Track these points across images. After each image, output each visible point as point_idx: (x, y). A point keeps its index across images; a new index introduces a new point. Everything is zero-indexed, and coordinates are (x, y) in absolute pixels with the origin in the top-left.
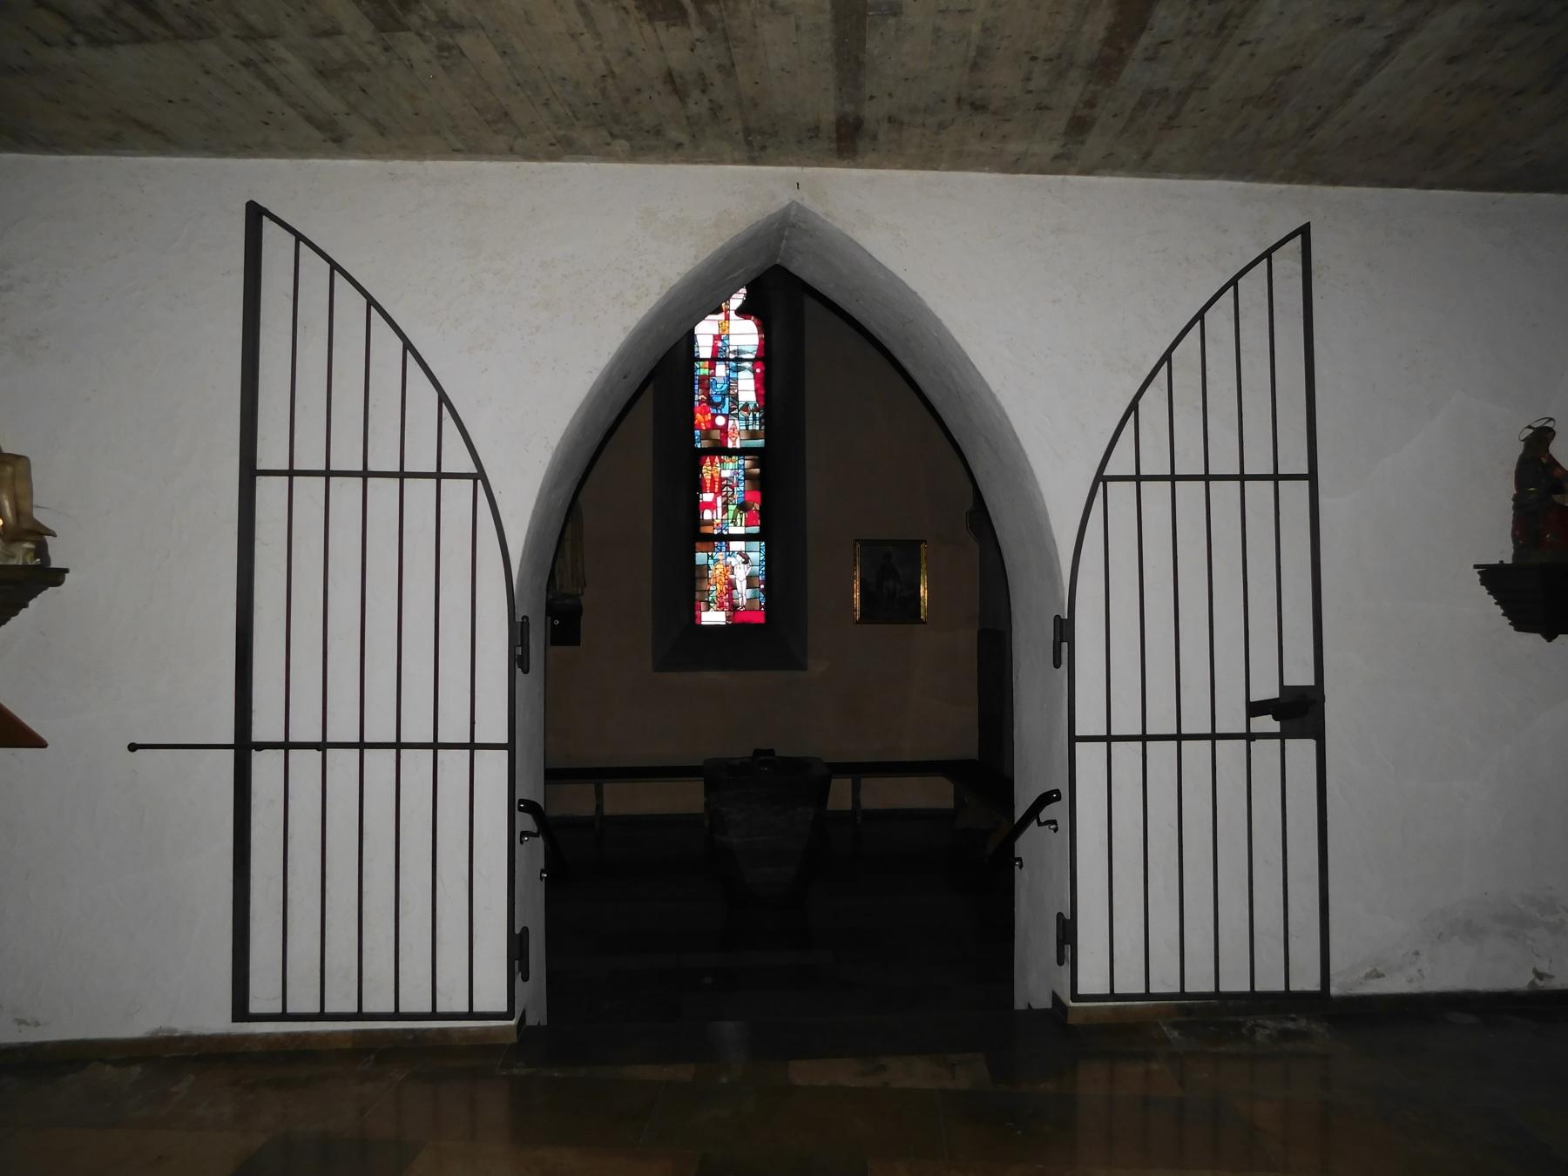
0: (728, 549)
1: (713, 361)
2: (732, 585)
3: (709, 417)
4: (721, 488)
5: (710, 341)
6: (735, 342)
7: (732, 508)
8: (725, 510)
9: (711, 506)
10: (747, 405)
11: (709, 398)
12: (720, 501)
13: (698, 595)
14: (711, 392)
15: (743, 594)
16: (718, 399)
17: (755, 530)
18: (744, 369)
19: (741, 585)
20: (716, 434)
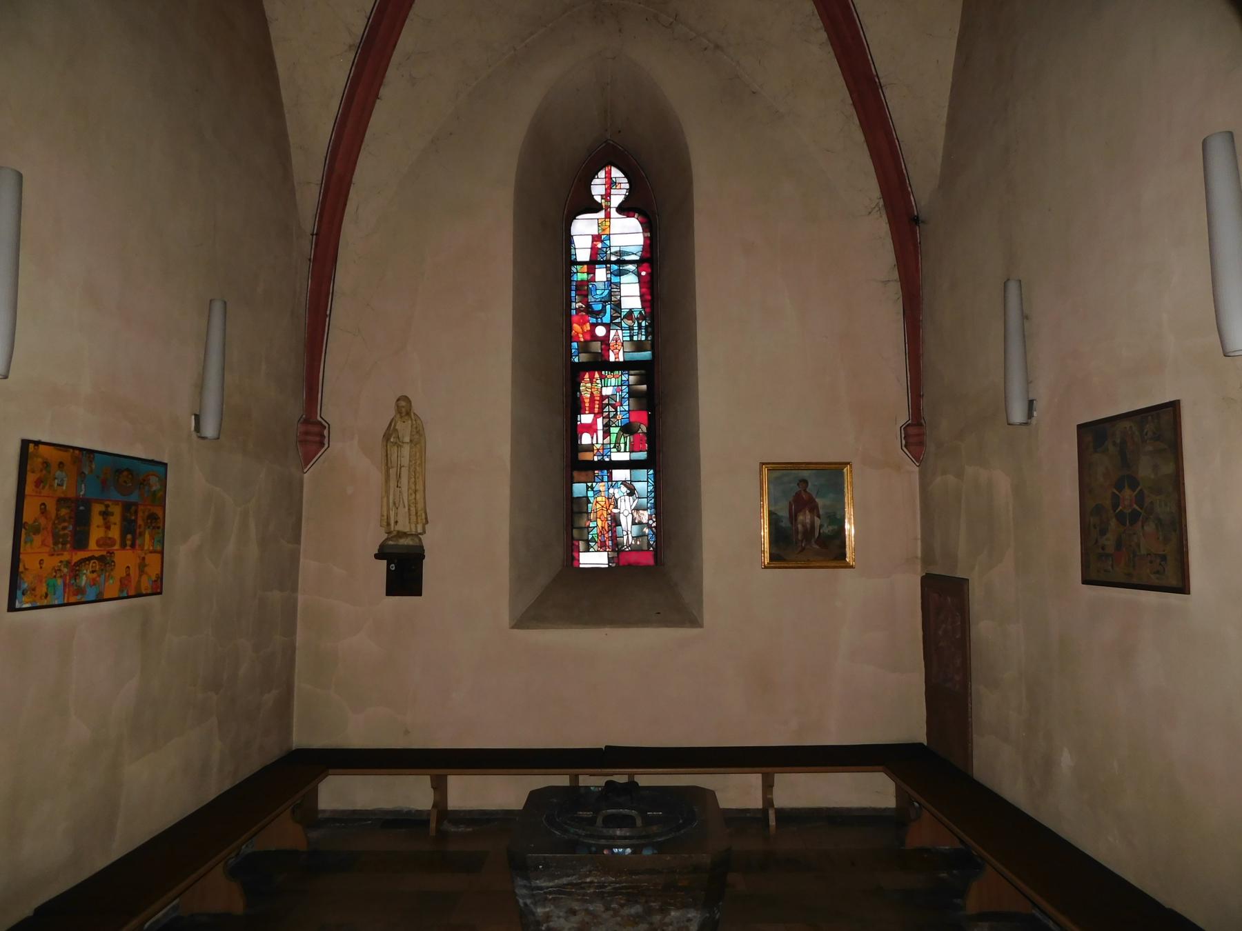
2: (616, 521)
3: (587, 327)
4: (602, 407)
5: (588, 242)
6: (617, 242)
7: (614, 430)
8: (607, 433)
9: (591, 429)
11: (588, 306)
12: (600, 421)
13: (575, 532)
14: (590, 299)
16: (598, 307)
17: (642, 455)
18: (627, 272)
19: (626, 521)
20: (596, 347)
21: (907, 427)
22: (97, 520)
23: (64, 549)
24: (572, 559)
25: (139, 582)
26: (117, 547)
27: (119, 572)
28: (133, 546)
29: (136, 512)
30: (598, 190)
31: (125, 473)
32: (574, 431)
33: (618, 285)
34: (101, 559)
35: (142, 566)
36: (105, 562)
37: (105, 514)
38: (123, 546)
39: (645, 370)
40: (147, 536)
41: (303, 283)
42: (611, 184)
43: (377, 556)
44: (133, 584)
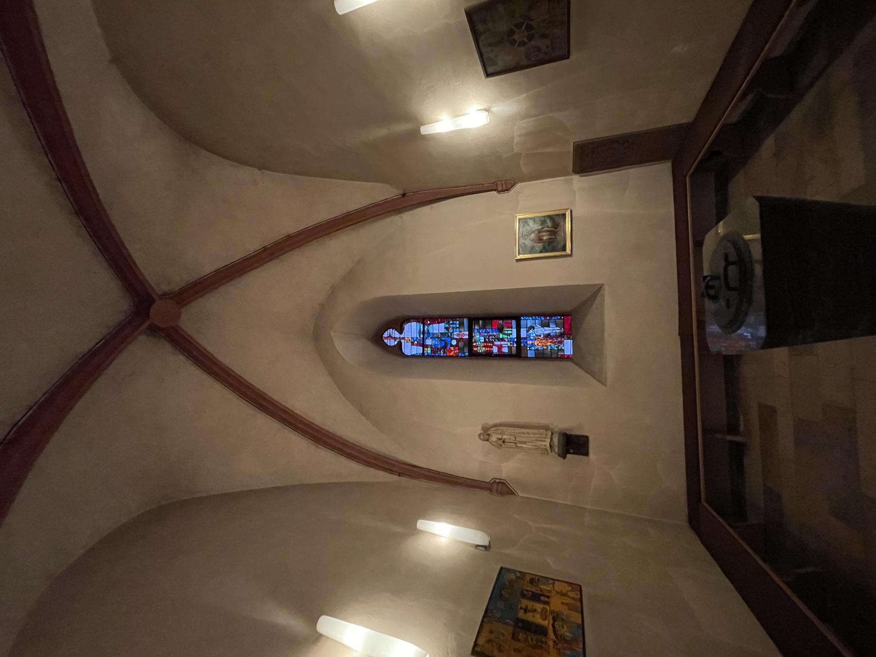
0: (525, 338)
1: (424, 346)
2: (548, 336)
3: (452, 348)
4: (490, 342)
6: (415, 335)
7: (501, 336)
8: (503, 340)
9: (500, 347)
10: (447, 329)
12: (497, 343)
13: (554, 356)
15: (554, 329)
17: (514, 322)
19: (547, 331)
20: (461, 344)
21: (499, 192)
22: (529, 617)
23: (546, 643)
24: (568, 358)
25: (573, 598)
26: (548, 608)
27: (564, 610)
28: (548, 597)
29: (528, 591)
30: (392, 343)
31: (503, 592)
32: (501, 356)
33: (433, 334)
34: (554, 619)
35: (562, 594)
36: (556, 617)
37: (526, 610)
38: (547, 603)
39: (473, 320)
40: (543, 587)
41: (423, 484)
42: (390, 337)
43: (564, 457)
44: (572, 602)
